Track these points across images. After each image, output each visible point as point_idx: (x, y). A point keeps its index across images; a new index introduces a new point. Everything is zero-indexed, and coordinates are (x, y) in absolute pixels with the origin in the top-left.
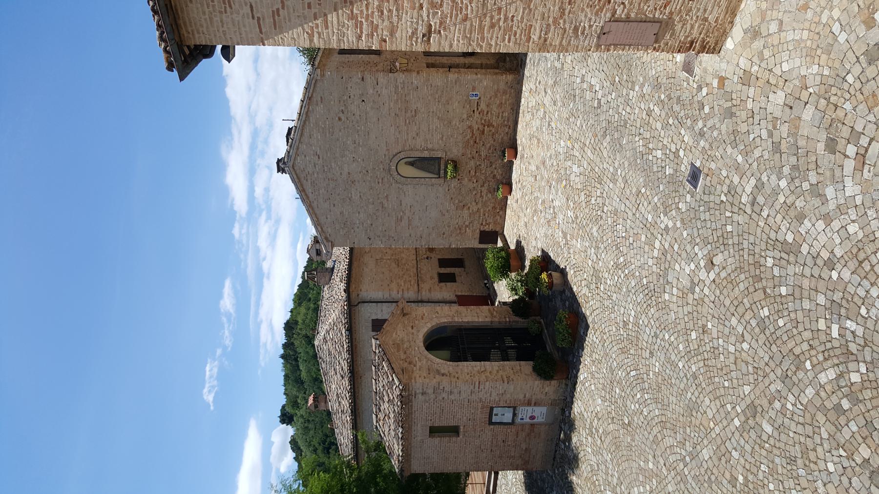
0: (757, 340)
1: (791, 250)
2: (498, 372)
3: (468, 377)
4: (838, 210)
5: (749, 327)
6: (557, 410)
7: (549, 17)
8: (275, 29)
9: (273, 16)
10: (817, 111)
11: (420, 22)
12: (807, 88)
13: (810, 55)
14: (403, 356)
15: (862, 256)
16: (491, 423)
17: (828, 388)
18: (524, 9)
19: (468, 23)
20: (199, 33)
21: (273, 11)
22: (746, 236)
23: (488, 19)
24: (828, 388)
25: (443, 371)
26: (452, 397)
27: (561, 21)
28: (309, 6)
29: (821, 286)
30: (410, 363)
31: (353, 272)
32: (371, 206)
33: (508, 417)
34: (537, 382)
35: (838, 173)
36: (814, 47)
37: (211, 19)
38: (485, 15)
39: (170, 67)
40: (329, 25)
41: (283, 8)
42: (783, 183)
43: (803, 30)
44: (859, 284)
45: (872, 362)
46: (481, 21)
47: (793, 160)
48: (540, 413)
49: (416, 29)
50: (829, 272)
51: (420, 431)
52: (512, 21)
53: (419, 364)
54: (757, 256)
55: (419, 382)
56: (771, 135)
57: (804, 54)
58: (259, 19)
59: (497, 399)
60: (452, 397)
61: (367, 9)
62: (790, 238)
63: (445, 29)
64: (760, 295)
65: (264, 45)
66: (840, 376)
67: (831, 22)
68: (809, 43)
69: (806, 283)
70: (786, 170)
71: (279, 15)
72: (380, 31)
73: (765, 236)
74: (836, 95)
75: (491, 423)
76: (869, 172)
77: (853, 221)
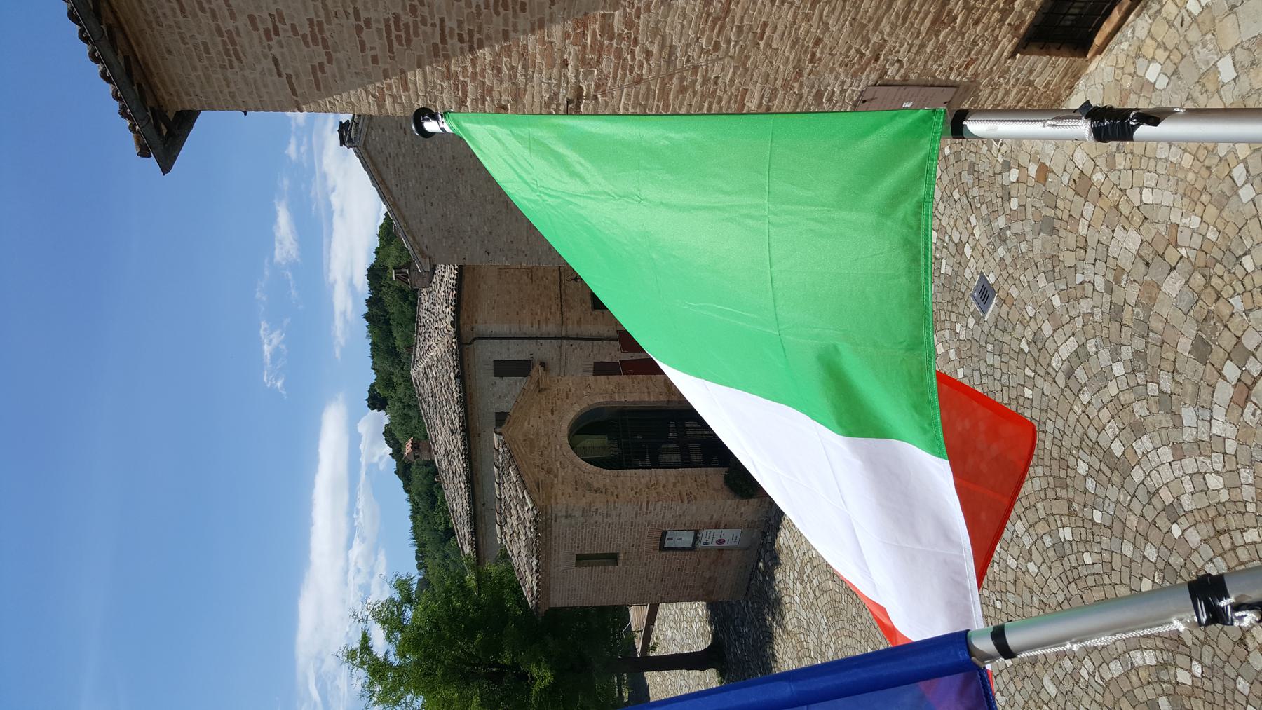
0: (1050, 567)
1: (1119, 467)
2: (674, 485)
3: (631, 494)
4: (1195, 447)
5: (1039, 544)
6: (756, 533)
7: (776, 79)
8: (319, 89)
9: (314, 73)
10: (1186, 289)
11: (563, 84)
12: (1176, 246)
13: (1191, 196)
15: (1221, 524)
16: (662, 548)
17: (1143, 674)
18: (736, 68)
19: (643, 87)
20: (188, 94)
21: (313, 67)
22: (1052, 415)
23: (675, 81)
24: (1143, 674)
25: (596, 485)
26: (609, 520)
27: (796, 85)
28: (375, 60)
29: (1153, 534)
30: (549, 472)
31: (465, 291)
32: (488, 207)
33: (686, 539)
34: (729, 502)
35: (1205, 393)
36: (1199, 186)
37: (208, 77)
38: (671, 76)
39: (144, 153)
40: (410, 85)
41: (330, 61)
42: (1119, 369)
43: (1185, 151)
44: (1211, 560)
45: (1211, 667)
46: (664, 84)
47: (1139, 343)
48: (731, 537)
49: (557, 94)
50: (1168, 523)
51: (562, 560)
52: (716, 83)
53: (561, 473)
54: (1064, 450)
55: (561, 505)
56: (1109, 289)
57: (1181, 191)
58: (289, 77)
59: (672, 521)
60: (609, 520)
61: (474, 65)
62: (1117, 449)
63: (604, 94)
64: (1061, 507)
65: (301, 110)
66: (1163, 665)
67: (1231, 158)
68: (1191, 177)
69: (1132, 521)
70: (1126, 352)
71: (323, 72)
72: (495, 95)
73: (1080, 430)
74: (1221, 277)
75: (662, 548)
76: (1254, 414)
77: (1217, 473)
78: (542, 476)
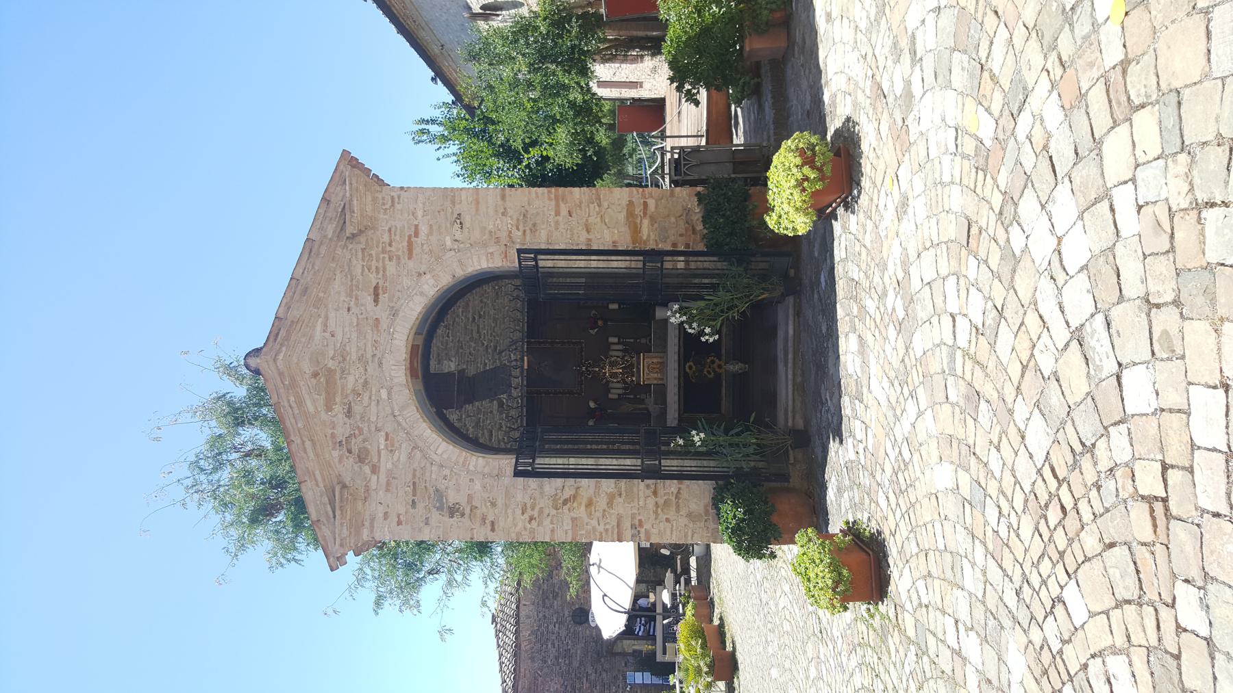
14: (341, 432)
25: (452, 498)
30: (361, 460)
53: (386, 464)
78: (347, 469)
